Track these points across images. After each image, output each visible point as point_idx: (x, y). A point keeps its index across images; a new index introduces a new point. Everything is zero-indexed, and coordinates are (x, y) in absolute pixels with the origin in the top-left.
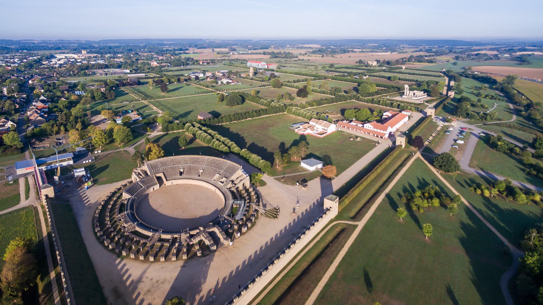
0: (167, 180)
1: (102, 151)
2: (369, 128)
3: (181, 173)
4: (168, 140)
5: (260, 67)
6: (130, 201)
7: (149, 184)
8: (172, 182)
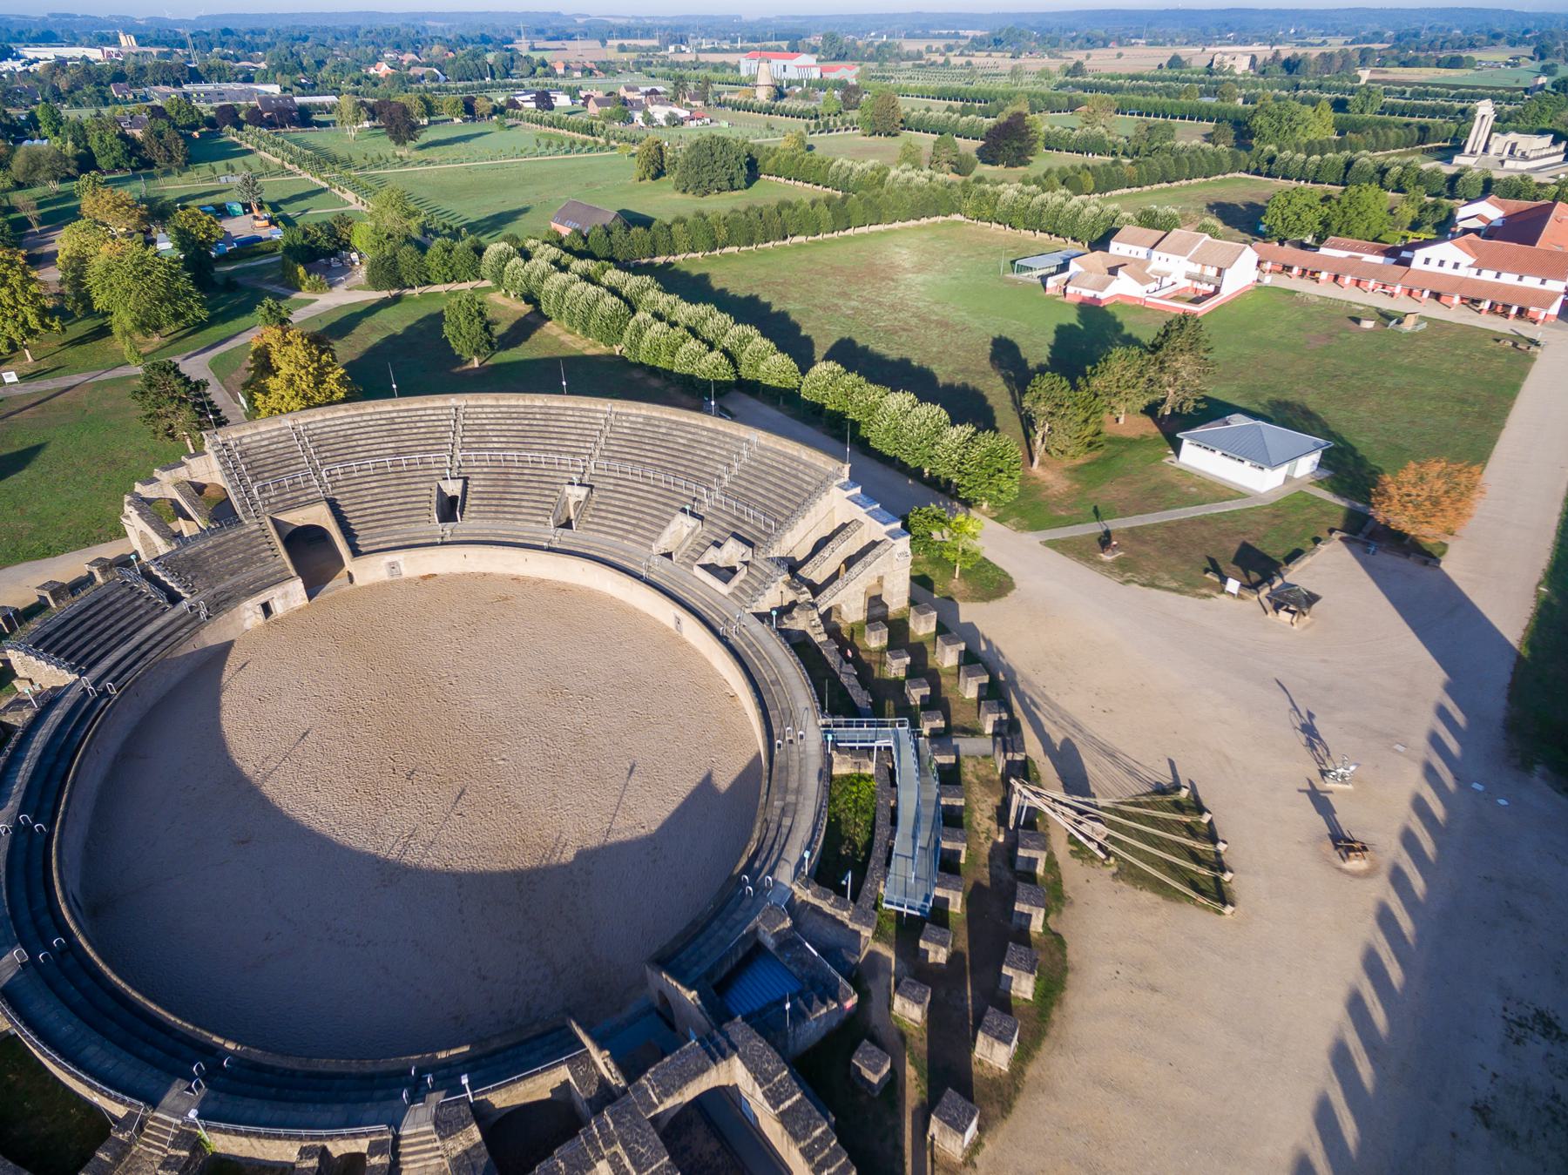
0: (356, 552)
1: (23, 378)
2: (1448, 269)
3: (449, 509)
4: (398, 328)
5: (792, 74)
6: (56, 716)
7: (233, 580)
8: (393, 566)
